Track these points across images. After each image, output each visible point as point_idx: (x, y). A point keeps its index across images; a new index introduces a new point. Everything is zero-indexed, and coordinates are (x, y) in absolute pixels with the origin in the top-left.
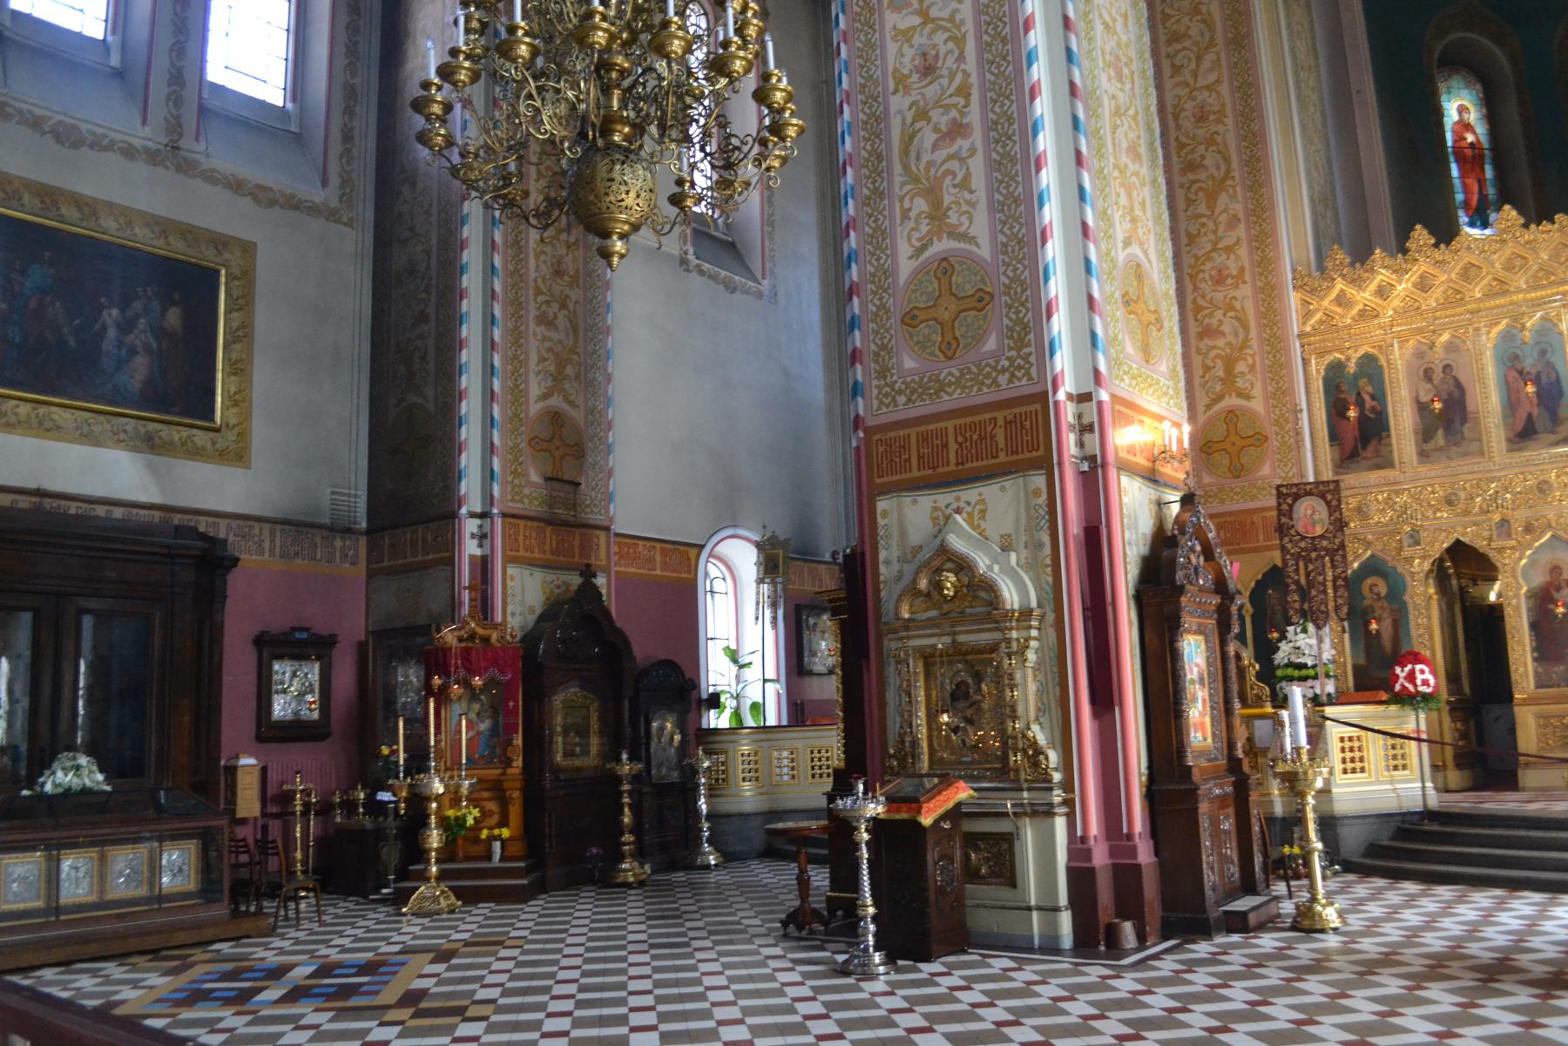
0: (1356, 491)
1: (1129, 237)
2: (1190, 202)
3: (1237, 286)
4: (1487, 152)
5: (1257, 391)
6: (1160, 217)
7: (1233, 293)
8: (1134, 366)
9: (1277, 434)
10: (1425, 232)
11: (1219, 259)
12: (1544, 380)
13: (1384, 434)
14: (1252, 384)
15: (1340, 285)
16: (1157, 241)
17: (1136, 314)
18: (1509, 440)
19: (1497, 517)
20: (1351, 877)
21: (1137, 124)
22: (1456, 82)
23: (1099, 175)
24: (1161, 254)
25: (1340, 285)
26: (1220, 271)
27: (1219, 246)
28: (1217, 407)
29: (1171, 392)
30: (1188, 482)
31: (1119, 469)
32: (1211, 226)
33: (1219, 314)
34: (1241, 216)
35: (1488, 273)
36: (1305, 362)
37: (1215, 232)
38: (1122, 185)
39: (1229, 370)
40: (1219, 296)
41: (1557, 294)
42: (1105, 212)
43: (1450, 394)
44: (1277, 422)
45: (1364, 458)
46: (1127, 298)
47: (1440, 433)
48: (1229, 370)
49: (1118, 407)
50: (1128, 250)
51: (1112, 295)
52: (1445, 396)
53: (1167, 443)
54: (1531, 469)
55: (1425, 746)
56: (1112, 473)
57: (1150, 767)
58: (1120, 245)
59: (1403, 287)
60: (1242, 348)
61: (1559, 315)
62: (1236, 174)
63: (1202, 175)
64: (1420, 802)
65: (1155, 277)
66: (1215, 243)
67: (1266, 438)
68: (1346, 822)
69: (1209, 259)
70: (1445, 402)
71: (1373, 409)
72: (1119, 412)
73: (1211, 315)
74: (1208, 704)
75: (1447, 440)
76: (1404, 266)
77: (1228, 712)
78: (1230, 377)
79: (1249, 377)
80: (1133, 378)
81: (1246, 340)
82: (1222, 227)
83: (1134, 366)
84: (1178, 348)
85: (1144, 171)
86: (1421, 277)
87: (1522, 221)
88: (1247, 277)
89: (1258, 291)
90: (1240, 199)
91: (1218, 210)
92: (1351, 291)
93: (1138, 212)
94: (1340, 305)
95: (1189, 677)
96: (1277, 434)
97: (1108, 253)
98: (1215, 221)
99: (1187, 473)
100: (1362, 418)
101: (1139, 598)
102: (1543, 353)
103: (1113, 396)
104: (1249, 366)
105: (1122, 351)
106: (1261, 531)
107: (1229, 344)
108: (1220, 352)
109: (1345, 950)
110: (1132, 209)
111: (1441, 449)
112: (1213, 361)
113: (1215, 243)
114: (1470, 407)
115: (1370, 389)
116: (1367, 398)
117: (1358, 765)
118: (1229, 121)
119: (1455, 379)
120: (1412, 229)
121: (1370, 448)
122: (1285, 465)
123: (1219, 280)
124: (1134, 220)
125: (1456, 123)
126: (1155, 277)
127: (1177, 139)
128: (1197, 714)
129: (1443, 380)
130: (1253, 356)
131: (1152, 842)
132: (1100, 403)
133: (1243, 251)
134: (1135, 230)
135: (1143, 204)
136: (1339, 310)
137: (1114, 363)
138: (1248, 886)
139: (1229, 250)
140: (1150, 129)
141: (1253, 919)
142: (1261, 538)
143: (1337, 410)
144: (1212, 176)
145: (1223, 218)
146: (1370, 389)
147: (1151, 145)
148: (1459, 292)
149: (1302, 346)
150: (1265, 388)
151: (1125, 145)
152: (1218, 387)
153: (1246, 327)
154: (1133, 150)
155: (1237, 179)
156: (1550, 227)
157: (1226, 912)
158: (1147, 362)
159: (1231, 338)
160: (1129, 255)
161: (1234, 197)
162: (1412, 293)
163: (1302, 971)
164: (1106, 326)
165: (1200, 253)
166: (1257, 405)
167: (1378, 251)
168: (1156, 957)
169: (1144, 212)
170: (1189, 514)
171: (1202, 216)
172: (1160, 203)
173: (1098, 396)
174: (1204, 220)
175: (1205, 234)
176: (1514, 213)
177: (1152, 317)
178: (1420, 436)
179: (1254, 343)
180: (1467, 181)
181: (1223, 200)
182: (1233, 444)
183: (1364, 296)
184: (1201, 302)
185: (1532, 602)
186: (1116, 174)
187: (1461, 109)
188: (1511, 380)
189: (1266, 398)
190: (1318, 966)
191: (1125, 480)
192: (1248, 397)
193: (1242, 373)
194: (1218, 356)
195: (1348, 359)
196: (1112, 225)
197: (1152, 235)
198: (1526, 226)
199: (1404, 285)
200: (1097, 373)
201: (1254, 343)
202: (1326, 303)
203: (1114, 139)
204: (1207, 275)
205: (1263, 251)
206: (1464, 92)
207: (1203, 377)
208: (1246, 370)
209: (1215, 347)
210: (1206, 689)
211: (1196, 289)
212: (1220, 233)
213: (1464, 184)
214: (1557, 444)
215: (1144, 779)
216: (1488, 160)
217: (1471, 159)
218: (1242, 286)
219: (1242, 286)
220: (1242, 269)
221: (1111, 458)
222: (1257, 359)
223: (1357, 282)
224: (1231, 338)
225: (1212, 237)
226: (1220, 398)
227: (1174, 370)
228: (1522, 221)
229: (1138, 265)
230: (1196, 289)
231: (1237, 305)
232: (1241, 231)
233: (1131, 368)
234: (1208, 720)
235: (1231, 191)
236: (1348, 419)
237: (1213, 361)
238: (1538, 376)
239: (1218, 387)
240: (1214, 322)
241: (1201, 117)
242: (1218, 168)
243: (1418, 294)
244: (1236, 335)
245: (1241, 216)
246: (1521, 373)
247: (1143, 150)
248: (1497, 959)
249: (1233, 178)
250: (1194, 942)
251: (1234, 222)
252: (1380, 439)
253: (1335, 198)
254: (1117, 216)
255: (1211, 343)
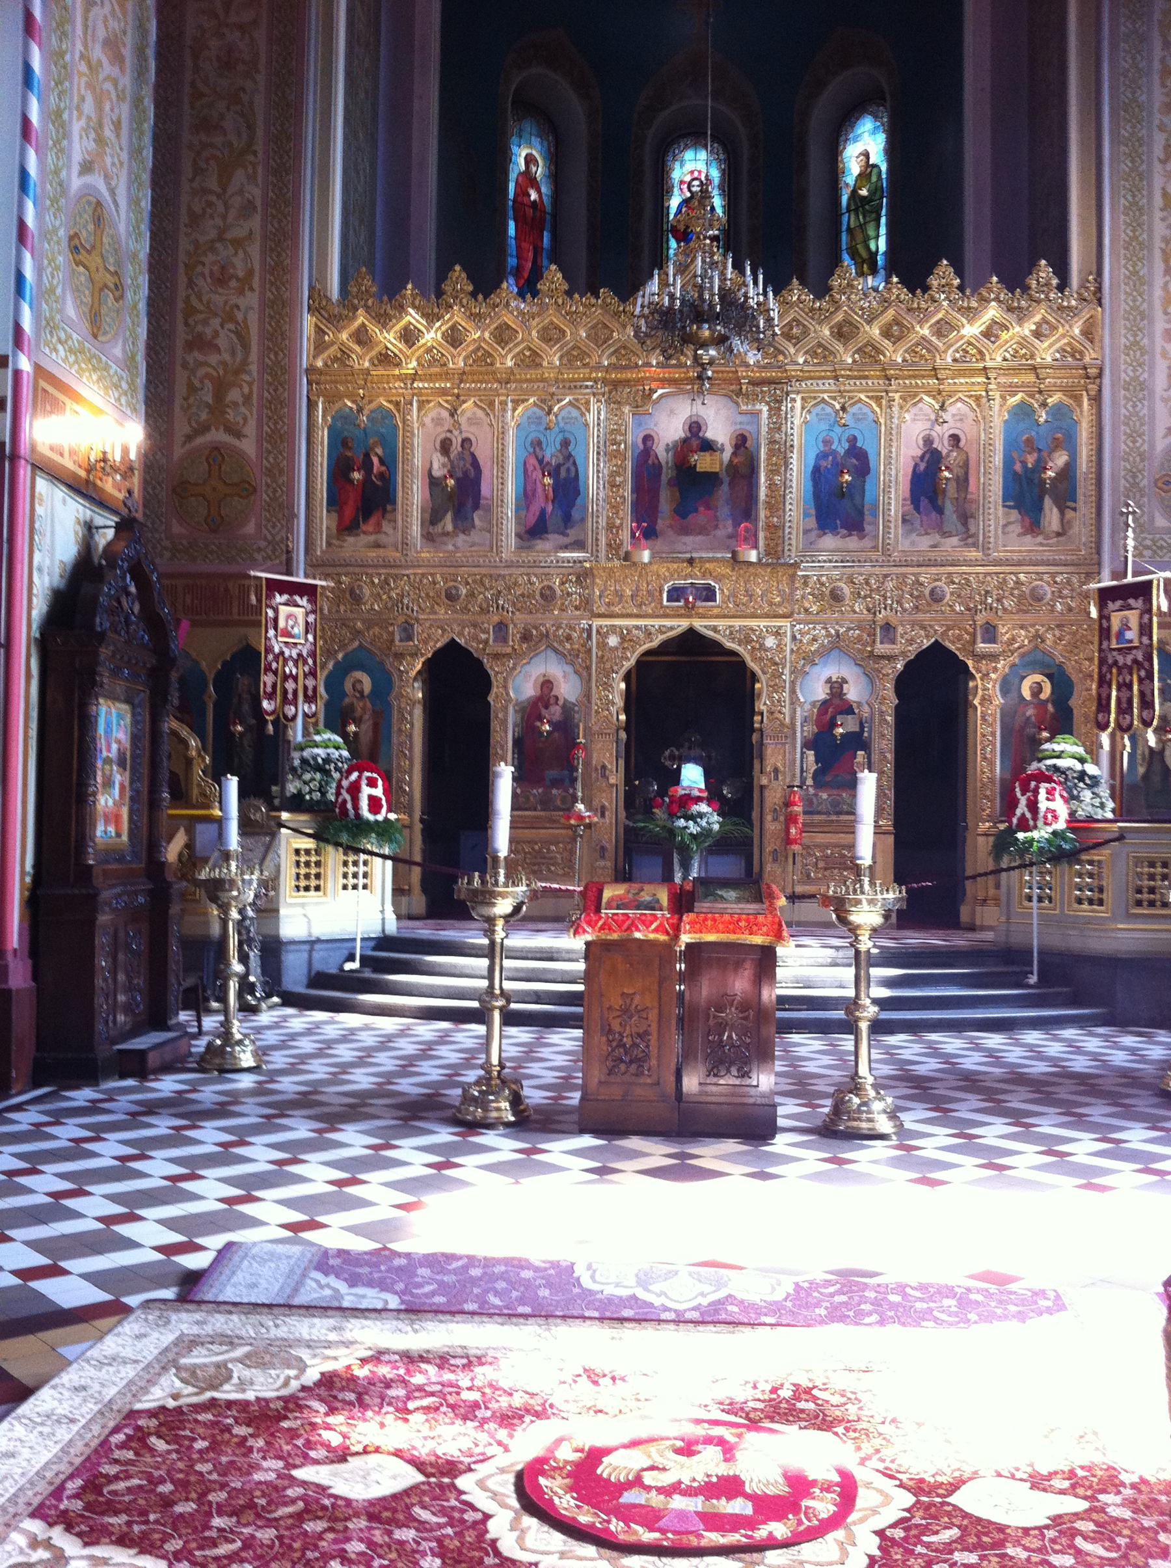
0: (351, 569)
1: (91, 162)
2: (197, 171)
3: (241, 292)
4: (548, 217)
5: (250, 429)
6: (139, 151)
7: (234, 300)
8: (75, 336)
9: (268, 486)
10: (464, 275)
11: (225, 252)
12: (563, 474)
13: (389, 507)
14: (245, 419)
15: (361, 318)
16: (130, 183)
17: (85, 267)
18: (518, 535)
19: (496, 619)
20: (290, 1011)
21: (124, 14)
22: (528, 126)
23: (54, 57)
24: (134, 202)
25: (361, 318)
26: (223, 268)
27: (228, 236)
28: (200, 440)
29: (124, 385)
30: (129, 503)
31: (35, 467)
32: (221, 208)
33: (215, 322)
34: (258, 203)
35: (523, 341)
36: (311, 405)
37: (224, 217)
38: (89, 86)
39: (219, 395)
40: (218, 300)
41: (589, 379)
42: (59, 113)
43: (466, 473)
44: (269, 472)
45: (365, 533)
46: (76, 241)
47: (449, 517)
48: (219, 395)
49: (43, 384)
50: (88, 179)
51: (55, 231)
52: (460, 474)
53: (108, 450)
54: (537, 571)
55: (389, 863)
56: (25, 472)
57: (37, 865)
58: (76, 169)
59: (431, 336)
60: (237, 372)
61: (588, 403)
62: (259, 147)
63: (218, 140)
64: (379, 928)
65: (122, 228)
66: (221, 232)
67: (255, 490)
68: (292, 947)
69: (212, 249)
70: (458, 480)
71: (381, 476)
72: (44, 390)
73: (205, 322)
74: (128, 794)
75: (455, 527)
76: (436, 310)
77: (154, 804)
78: (219, 406)
79: (243, 409)
80: (71, 351)
81: (245, 362)
82: (233, 213)
83: (75, 336)
84: (142, 332)
85: (126, 81)
86: (453, 328)
87: (566, 287)
88: (256, 283)
89: (263, 304)
90: (260, 180)
91: (231, 190)
92: (374, 329)
93: (108, 132)
94: (359, 342)
95: (105, 754)
96: (268, 486)
97: (57, 172)
98: (225, 204)
99: (130, 492)
100: (367, 480)
101: (45, 644)
102: (566, 443)
103: (38, 368)
104: (243, 395)
105: (61, 311)
106: (235, 603)
107: (224, 364)
108: (210, 370)
109: (259, 1090)
110: (100, 125)
111: (447, 534)
112: (202, 382)
113: (221, 232)
114: (485, 490)
115: (379, 451)
116: (375, 460)
117: (313, 883)
118: (261, 78)
119: (473, 455)
120: (450, 268)
121: (373, 520)
122: (274, 527)
123: (222, 279)
124: (100, 141)
125: (520, 174)
126: (122, 228)
127: (193, 84)
128: (110, 802)
129: (461, 456)
130: (250, 384)
131: (29, 962)
132: (17, 373)
133: (255, 250)
134: (101, 155)
135: (117, 125)
136: (357, 348)
137: (44, 323)
138: (158, 1019)
139: (237, 243)
140: (142, 29)
141: (153, 1060)
142: (235, 610)
143: (339, 470)
144: (230, 144)
145: (237, 201)
146: (379, 451)
147: (140, 52)
148: (490, 355)
149: (309, 383)
150: (260, 426)
151: (101, 33)
152: (204, 416)
153: (246, 347)
154: (112, 45)
155: (260, 155)
156: (593, 301)
157: (120, 1051)
158: (95, 336)
159: (226, 356)
160: (87, 186)
161: (252, 178)
162: (440, 345)
163: (198, 1115)
164: (39, 270)
165: (202, 239)
166: (248, 446)
167: (410, 286)
168: (18, 1108)
169: (118, 136)
170: (123, 544)
171: (205, 191)
172: (142, 133)
173: (15, 362)
174: (214, 199)
175: (212, 217)
176: (560, 275)
177: (110, 280)
178: (427, 516)
179: (254, 368)
180: (524, 245)
181: (239, 176)
182: (214, 489)
183: (389, 338)
184: (195, 302)
185: (519, 716)
186: (83, 67)
187: (529, 159)
188: (530, 468)
189: (260, 440)
190: (220, 1111)
191: (42, 485)
192: (238, 435)
193: (236, 404)
194: (207, 375)
195: (360, 410)
196: (67, 135)
197: (124, 172)
198: (569, 293)
199: (432, 334)
200: (18, 330)
201: (254, 368)
202: (344, 336)
203: (86, 19)
204: (207, 272)
205: (279, 255)
206: (536, 141)
207: (186, 399)
208: (240, 400)
209: (206, 364)
210: (127, 773)
211: (191, 284)
212: (230, 220)
213: (518, 247)
214: (565, 548)
215: (28, 879)
216: (548, 225)
217: (530, 218)
218: (248, 293)
219: (248, 293)
220: (250, 273)
221: (24, 450)
222: (255, 389)
223: (383, 320)
224: (226, 356)
225: (218, 221)
226: (204, 429)
227: (133, 358)
228: (566, 287)
229: (99, 204)
230: (191, 284)
231: (240, 316)
232: (255, 222)
233: (69, 337)
234: (125, 812)
235: (250, 171)
236: (351, 481)
237: (202, 382)
238: (559, 466)
239: (204, 416)
240: (208, 331)
241: (227, 63)
242: (239, 134)
243: (448, 350)
244: (233, 353)
245: (258, 203)
246: (541, 462)
247: (127, 52)
248: (428, 1095)
249: (255, 153)
250: (77, 1087)
251: (248, 208)
252: (385, 511)
253: (373, 215)
254: (77, 127)
255: (201, 358)
